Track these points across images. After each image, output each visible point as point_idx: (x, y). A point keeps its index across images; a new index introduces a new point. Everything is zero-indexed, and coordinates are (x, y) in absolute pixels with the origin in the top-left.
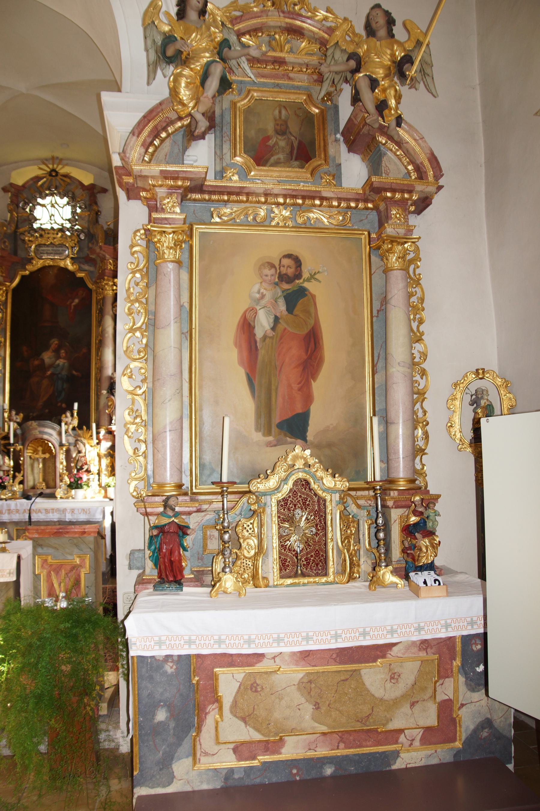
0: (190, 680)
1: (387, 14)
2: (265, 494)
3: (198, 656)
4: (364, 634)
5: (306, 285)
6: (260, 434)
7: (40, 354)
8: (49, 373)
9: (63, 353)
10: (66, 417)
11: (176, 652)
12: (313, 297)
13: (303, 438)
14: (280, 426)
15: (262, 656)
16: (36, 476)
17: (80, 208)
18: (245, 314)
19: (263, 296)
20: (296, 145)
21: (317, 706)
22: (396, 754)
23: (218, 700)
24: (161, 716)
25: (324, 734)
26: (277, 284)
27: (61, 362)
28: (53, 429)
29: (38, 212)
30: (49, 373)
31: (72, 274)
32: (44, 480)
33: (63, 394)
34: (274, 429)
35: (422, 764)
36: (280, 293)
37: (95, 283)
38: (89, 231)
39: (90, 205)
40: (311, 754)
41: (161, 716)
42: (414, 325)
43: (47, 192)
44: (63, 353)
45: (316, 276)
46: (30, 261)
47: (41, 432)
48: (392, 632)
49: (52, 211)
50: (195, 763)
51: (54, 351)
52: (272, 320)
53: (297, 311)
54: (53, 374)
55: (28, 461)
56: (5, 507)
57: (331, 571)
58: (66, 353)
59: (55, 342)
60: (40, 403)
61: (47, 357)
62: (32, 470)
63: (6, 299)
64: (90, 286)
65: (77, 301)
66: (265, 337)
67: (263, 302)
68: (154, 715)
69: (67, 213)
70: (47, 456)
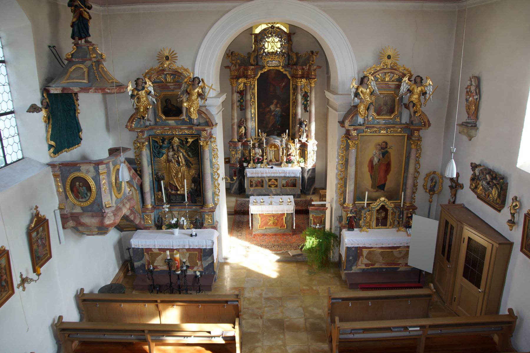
0: (357, 251)
1: (421, 78)
2: (374, 208)
3: (360, 247)
4: (395, 244)
5: (388, 150)
6: (372, 189)
7: (270, 106)
8: (273, 114)
9: (278, 105)
10: (283, 135)
11: (355, 246)
12: (390, 153)
13: (384, 190)
14: (378, 187)
15: (373, 247)
16: (271, 156)
17: (284, 42)
18: (371, 158)
19: (376, 153)
20: (389, 109)
21: (383, 258)
22: (399, 268)
23: (362, 255)
24: (351, 258)
25: (384, 263)
26: (380, 150)
27: (278, 109)
28: (279, 140)
29: (266, 45)
30: (273, 114)
31: (282, 72)
32: (274, 158)
33: (279, 122)
34: (377, 188)
35: (405, 270)
36: (381, 152)
37: (292, 77)
38: (288, 53)
39: (288, 41)
40: (381, 267)
41: (351, 258)
42: (417, 159)
43: (270, 35)
44: (278, 105)
45: (392, 147)
46: (264, 67)
47: (274, 141)
48: (401, 244)
49: (273, 44)
50: (357, 267)
51: (275, 105)
52: (378, 160)
53: (385, 157)
54: (275, 114)
55: (268, 151)
56: (265, 172)
57: (388, 225)
58: (280, 106)
59: (275, 101)
60: (270, 126)
61: (272, 107)
62: (270, 154)
63: (255, 84)
64: (290, 78)
65: (284, 84)
66: (376, 164)
67: (376, 155)
68: (349, 258)
69: (279, 45)
70: (276, 149)
